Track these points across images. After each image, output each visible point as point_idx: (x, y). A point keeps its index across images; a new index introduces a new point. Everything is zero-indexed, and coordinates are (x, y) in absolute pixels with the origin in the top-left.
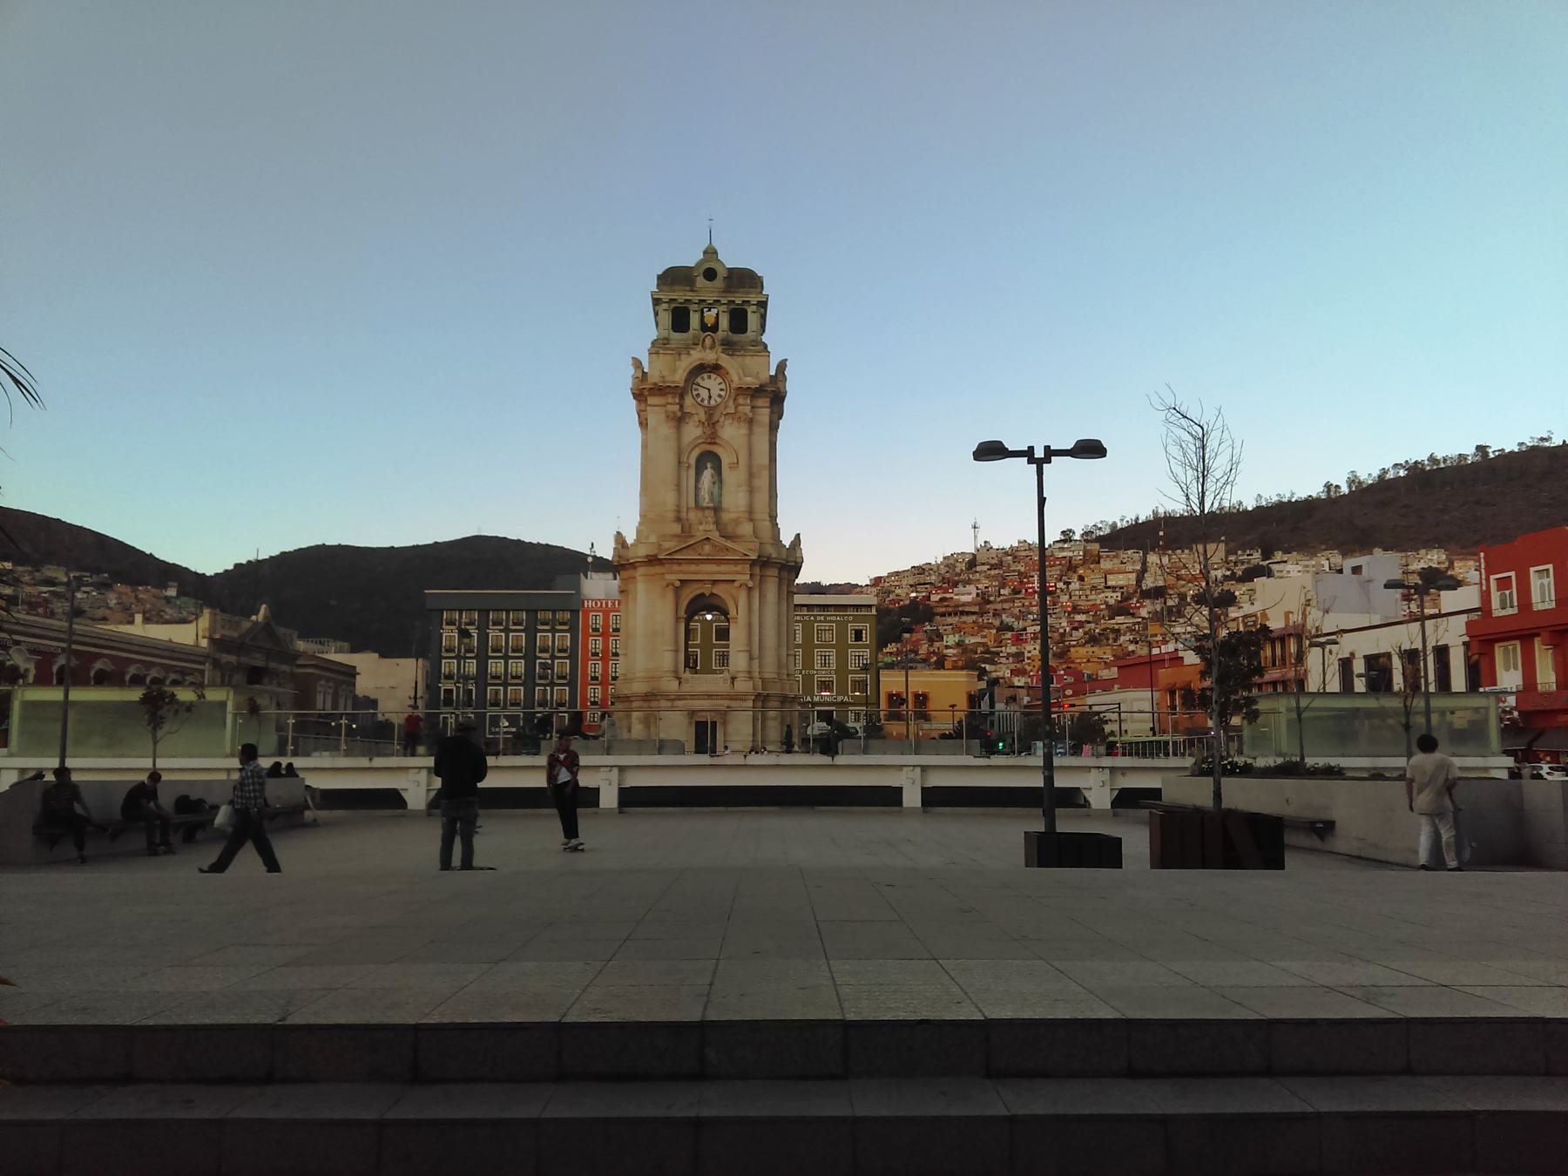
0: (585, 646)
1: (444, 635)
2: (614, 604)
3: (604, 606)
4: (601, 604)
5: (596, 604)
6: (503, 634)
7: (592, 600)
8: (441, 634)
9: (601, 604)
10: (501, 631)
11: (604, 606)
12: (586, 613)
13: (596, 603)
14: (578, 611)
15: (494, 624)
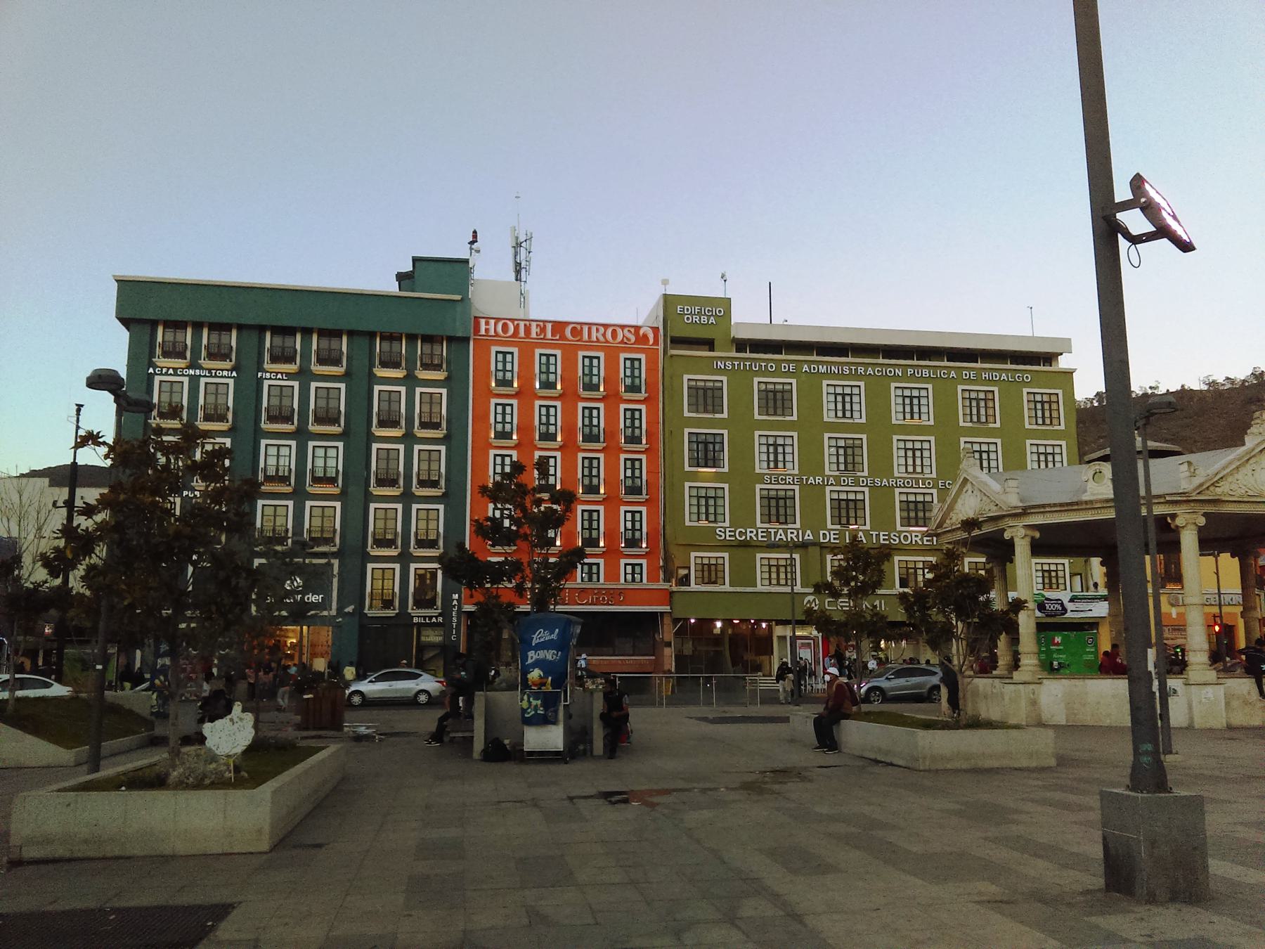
0: (482, 417)
1: (157, 379)
2: (543, 330)
3: (522, 333)
4: (517, 328)
5: (505, 327)
6: (296, 384)
7: (497, 320)
8: (150, 378)
9: (517, 328)
10: (290, 376)
11: (522, 333)
12: (484, 344)
13: (505, 327)
14: (467, 340)
15: (274, 360)
